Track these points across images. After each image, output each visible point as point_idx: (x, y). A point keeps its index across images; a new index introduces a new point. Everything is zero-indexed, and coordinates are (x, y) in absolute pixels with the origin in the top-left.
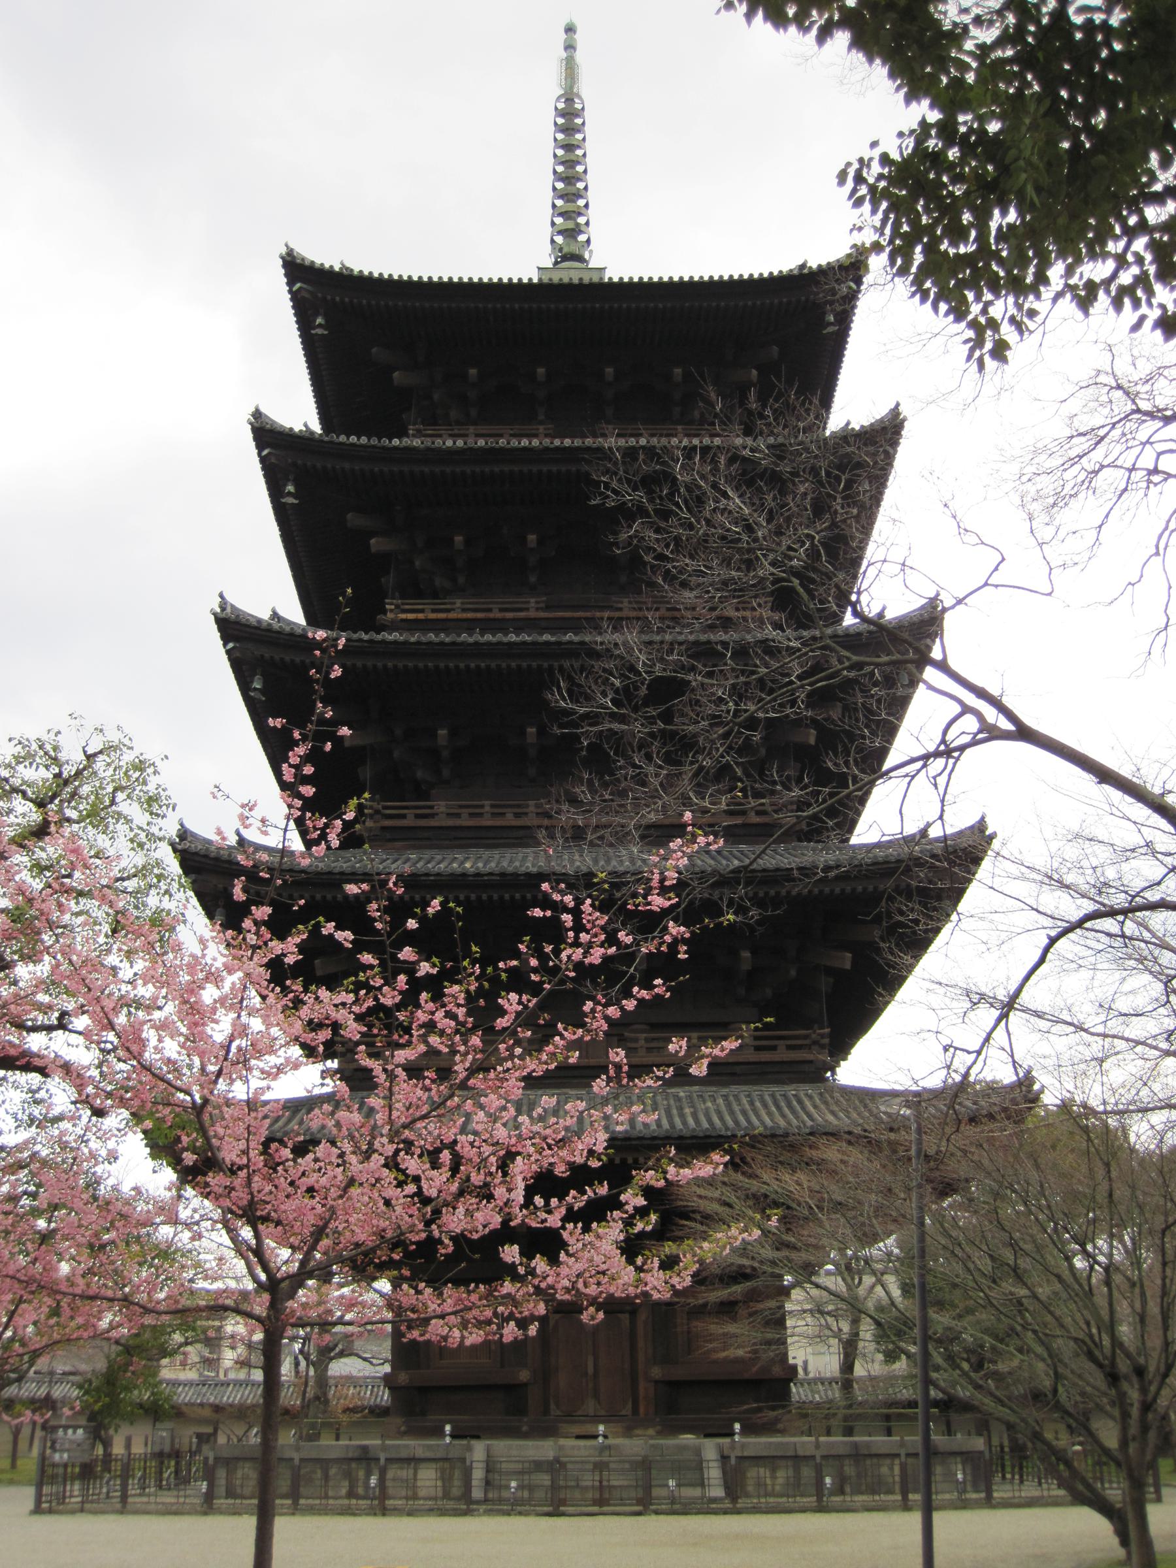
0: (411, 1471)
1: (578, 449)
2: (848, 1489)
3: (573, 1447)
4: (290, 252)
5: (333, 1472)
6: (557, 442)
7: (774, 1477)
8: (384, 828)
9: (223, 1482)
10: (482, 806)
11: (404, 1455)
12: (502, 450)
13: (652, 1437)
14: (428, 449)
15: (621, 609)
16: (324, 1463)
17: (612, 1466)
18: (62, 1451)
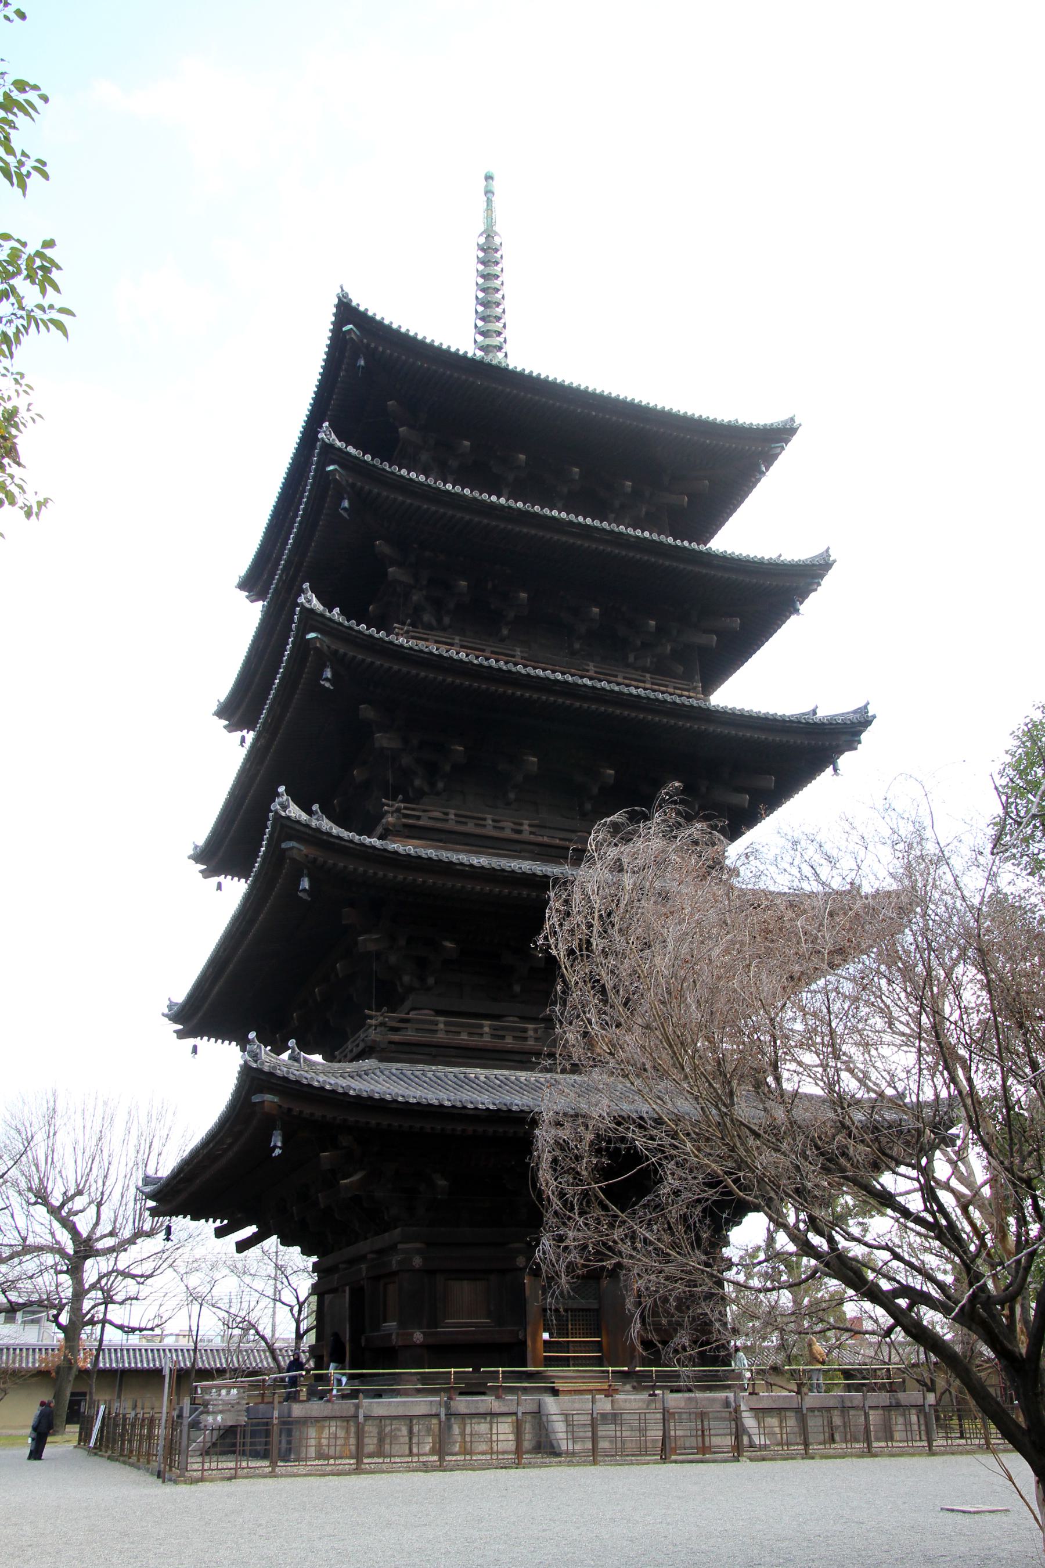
0: (488, 1426)
1: (596, 528)
2: (837, 1437)
3: (626, 1400)
4: (346, 296)
5: (415, 1429)
6: (581, 519)
7: (781, 1427)
8: (405, 825)
9: (313, 1442)
10: (485, 819)
11: (482, 1411)
12: (536, 514)
13: (627, 1392)
14: (475, 499)
15: (588, 671)
16: (410, 1419)
17: (711, 1415)
18: (213, 1413)
